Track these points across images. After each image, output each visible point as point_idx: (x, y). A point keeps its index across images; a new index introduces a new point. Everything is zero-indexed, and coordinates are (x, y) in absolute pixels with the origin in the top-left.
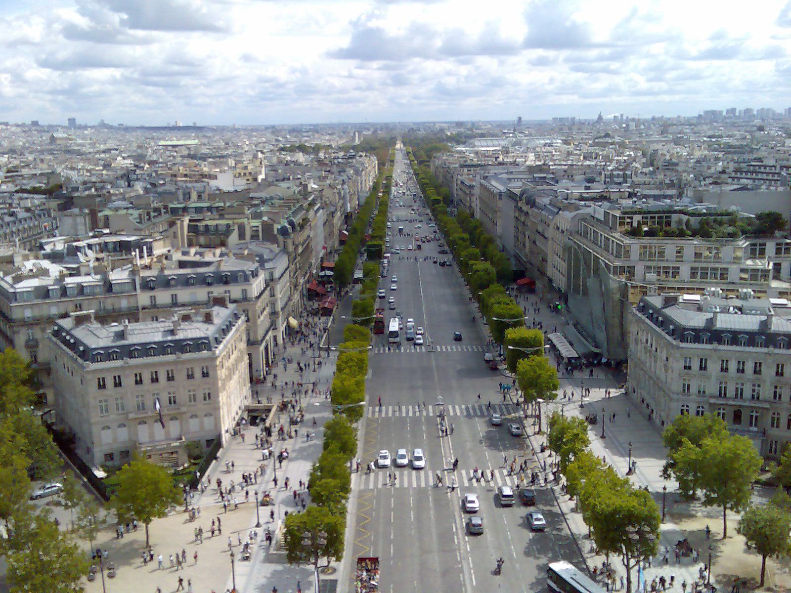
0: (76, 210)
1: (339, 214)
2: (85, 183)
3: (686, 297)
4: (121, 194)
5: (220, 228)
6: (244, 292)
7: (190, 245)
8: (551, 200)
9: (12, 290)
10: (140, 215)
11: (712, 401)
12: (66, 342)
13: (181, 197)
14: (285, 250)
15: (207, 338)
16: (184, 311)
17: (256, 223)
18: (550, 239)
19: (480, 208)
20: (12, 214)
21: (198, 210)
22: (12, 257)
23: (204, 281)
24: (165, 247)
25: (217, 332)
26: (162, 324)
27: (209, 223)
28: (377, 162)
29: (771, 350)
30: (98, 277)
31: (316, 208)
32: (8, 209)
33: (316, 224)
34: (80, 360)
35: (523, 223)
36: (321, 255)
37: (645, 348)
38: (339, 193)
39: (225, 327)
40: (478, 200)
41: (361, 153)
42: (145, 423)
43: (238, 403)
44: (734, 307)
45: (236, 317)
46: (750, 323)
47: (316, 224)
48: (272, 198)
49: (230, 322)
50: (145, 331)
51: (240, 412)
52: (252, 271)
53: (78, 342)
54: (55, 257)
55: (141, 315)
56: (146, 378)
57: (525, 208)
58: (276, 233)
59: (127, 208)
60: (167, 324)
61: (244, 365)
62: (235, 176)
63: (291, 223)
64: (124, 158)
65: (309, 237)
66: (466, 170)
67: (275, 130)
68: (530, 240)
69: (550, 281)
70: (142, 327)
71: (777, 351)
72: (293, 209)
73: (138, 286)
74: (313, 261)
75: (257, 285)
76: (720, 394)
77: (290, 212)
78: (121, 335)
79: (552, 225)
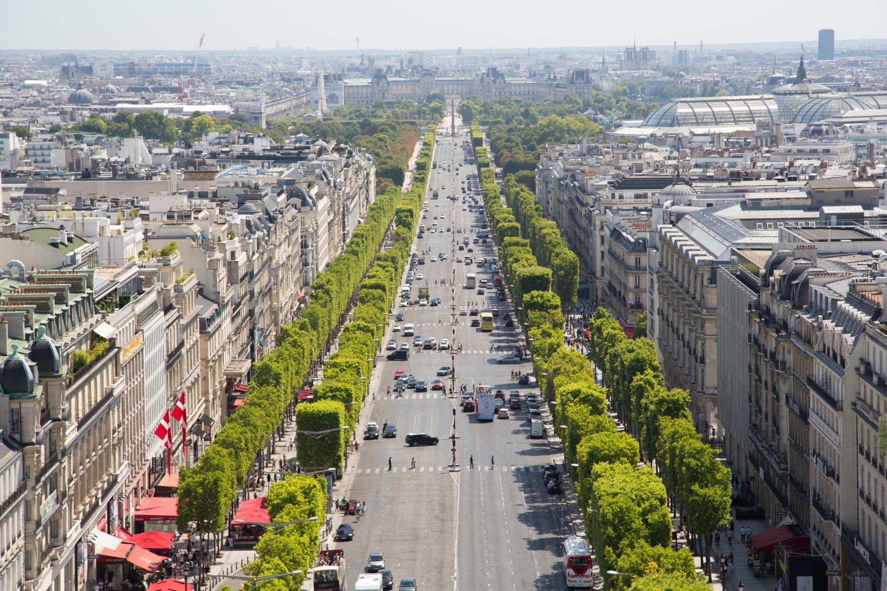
1: (227, 327)
8: (853, 287)
18: (847, 407)
19: (661, 313)
28: (373, 170)
31: (140, 307)
35: (773, 356)
38: (232, 266)
41: (321, 142)
47: (140, 353)
57: (779, 309)
63: (42, 356)
65: (110, 395)
66: (629, 194)
67: (73, 69)
68: (792, 410)
69: (850, 535)
72: (57, 310)
74: (122, 471)
77: (44, 319)
79: (852, 362)
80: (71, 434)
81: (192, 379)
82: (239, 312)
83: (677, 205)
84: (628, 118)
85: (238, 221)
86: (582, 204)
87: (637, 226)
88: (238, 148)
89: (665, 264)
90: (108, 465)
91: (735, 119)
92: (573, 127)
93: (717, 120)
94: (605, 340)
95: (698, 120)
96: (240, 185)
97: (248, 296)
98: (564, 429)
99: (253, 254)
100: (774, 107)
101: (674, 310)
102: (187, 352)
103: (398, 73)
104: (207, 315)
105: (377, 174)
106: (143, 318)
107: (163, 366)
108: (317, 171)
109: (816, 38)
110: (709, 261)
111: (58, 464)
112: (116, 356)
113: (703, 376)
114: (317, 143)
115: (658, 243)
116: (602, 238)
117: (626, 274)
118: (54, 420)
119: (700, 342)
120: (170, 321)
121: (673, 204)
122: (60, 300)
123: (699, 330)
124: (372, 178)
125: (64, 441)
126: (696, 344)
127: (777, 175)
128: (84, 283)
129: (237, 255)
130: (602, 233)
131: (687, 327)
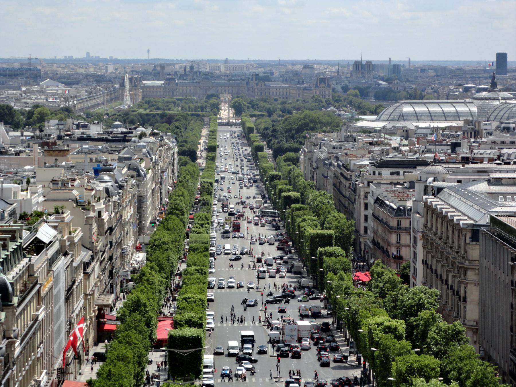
28: (176, 150)
40: (420, 243)
41: (141, 129)
47: (51, 289)
66: (386, 172)
81: (79, 309)
82: (104, 258)
83: (438, 181)
84: (364, 114)
85: (101, 189)
86: (346, 179)
87: (398, 197)
88: (78, 133)
89: (429, 225)
90: (34, 374)
91: (445, 116)
92: (323, 120)
93: (432, 116)
94: (386, 283)
95: (418, 117)
96: (94, 161)
97: (109, 246)
98: (374, 351)
99: (111, 213)
100: (474, 109)
101: (438, 261)
102: (76, 288)
103: (184, 76)
104: (86, 260)
105: (179, 154)
106: (52, 261)
107: (63, 298)
108: (144, 150)
109: (494, 59)
110: (471, 224)
111: (10, 371)
112: (39, 291)
113: (465, 312)
114: (138, 129)
115: (423, 211)
116: (366, 206)
117: (391, 232)
118: (8, 338)
119: (463, 286)
120: (68, 265)
121: (434, 180)
123: (462, 277)
124: (176, 156)
125: (14, 354)
126: (459, 287)
127: (496, 160)
128: (17, 235)
129: (102, 214)
130: (366, 201)
131: (450, 275)
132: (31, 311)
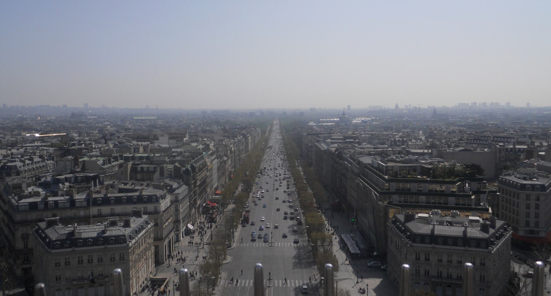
0: (70, 157)
2: (80, 141)
3: (420, 215)
4: (98, 148)
5: (150, 169)
6: (156, 208)
7: (131, 178)
9: (17, 204)
10: (104, 161)
11: (433, 280)
12: (41, 237)
13: (132, 150)
14: (187, 184)
15: (124, 236)
16: (112, 219)
17: (171, 167)
20: (31, 159)
21: (141, 158)
22: (21, 184)
23: (130, 200)
24: (110, 180)
25: (132, 232)
26: (98, 227)
27: (143, 166)
29: (467, 248)
30: (68, 197)
32: (30, 156)
33: (212, 167)
34: (46, 247)
36: (215, 186)
37: (396, 246)
38: (231, 150)
39: (137, 229)
42: (83, 287)
43: (145, 276)
44: (447, 222)
45: (147, 223)
46: (456, 231)
47: (212, 167)
48: (185, 152)
49: (142, 226)
50: (87, 231)
51: (145, 282)
52: (162, 196)
53: (47, 236)
54: (44, 185)
55: (92, 220)
56: (85, 258)
58: (182, 172)
59: (97, 156)
60: (101, 227)
61: (151, 253)
62: (170, 139)
63: (193, 167)
64: (111, 127)
65: (206, 175)
66: (310, 136)
70: (86, 228)
71: (470, 249)
73: (91, 203)
75: (164, 204)
76: (438, 276)
78: (72, 234)
80: (198, 183)
91: (331, 122)
122: (197, 157)
132: (205, 172)
